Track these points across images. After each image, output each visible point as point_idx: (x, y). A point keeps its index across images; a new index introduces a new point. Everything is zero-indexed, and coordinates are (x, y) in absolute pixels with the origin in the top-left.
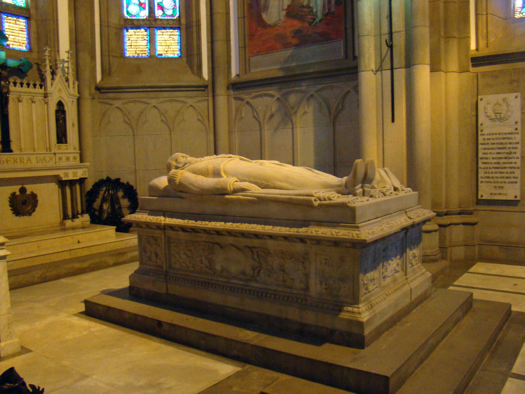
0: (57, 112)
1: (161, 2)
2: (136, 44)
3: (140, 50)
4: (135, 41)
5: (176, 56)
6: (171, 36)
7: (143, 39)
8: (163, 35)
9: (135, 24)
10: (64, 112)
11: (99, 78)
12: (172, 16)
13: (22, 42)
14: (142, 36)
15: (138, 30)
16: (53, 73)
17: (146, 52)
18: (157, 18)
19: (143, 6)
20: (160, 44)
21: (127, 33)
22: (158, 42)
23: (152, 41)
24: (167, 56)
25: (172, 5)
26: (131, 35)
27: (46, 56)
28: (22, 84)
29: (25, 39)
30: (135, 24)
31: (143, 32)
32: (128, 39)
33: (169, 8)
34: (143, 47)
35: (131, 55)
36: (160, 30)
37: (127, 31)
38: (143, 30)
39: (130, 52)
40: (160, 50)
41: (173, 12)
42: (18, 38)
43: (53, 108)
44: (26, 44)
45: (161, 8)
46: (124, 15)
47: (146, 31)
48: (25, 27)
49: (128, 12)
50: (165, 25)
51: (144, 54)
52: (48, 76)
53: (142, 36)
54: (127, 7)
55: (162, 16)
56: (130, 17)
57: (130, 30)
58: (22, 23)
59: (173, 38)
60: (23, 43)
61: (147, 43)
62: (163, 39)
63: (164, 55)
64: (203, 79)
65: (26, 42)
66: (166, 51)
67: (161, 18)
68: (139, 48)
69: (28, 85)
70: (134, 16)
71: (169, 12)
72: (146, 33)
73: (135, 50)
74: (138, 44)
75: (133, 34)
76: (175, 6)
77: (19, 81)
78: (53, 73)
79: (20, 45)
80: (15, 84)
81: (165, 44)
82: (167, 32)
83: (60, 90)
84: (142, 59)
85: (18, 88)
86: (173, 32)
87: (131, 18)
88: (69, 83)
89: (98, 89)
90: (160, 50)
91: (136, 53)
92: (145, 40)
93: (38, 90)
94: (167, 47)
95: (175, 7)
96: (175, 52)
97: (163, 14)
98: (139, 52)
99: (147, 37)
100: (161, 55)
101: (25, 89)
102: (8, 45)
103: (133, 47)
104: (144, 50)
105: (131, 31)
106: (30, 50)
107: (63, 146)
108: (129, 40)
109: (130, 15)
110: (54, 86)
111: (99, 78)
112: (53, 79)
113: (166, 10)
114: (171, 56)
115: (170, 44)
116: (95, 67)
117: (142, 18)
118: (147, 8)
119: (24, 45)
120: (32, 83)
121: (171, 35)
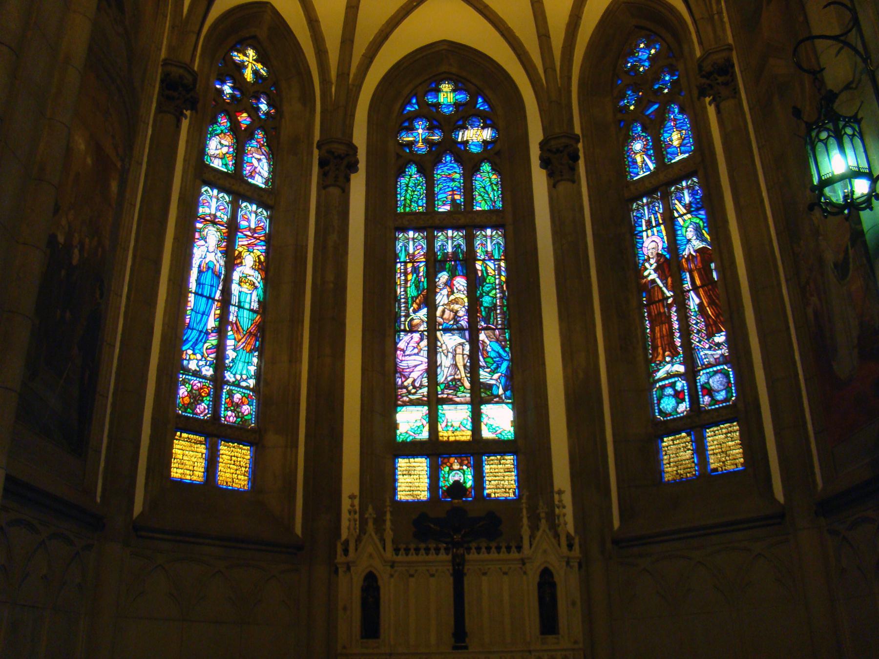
0: (540, 585)
1: (706, 383)
2: (676, 459)
3: (682, 467)
4: (674, 455)
5: (740, 468)
6: (729, 435)
7: (685, 449)
8: (715, 435)
9: (673, 427)
10: (553, 585)
11: (616, 524)
12: (726, 400)
13: (509, 487)
14: (684, 445)
15: (677, 436)
16: (534, 528)
17: (692, 470)
18: (703, 409)
19: (680, 396)
20: (711, 452)
21: (664, 444)
22: (710, 448)
23: (700, 449)
24: (725, 470)
25: (723, 383)
26: (667, 447)
27: (522, 503)
28: (488, 549)
29: (513, 482)
30: (673, 427)
31: (684, 437)
32: (664, 453)
33: (719, 389)
34: (687, 462)
35: (670, 478)
36: (708, 428)
37: (663, 441)
38: (684, 434)
39: (670, 472)
40: (714, 463)
41: (726, 394)
42: (503, 482)
43: (532, 579)
44: (515, 489)
45: (709, 391)
46: (655, 416)
47: (689, 434)
48: (512, 466)
49: (660, 411)
50: (717, 418)
51: (689, 473)
52: (525, 532)
53: (684, 445)
54: (659, 403)
55: (710, 405)
56: (663, 418)
57: (665, 439)
58: (508, 462)
59: (732, 438)
60: (509, 489)
61: (693, 454)
62: (715, 442)
63: (720, 469)
64: (776, 501)
65: (515, 486)
66: (723, 462)
67: (710, 408)
68: (681, 465)
69: (509, 549)
70: (670, 415)
71: (721, 396)
72: (689, 438)
73: (675, 469)
74: (679, 458)
75: (671, 443)
76: (729, 382)
77: (483, 545)
78: (534, 528)
79: (505, 492)
80: (478, 549)
81: (720, 450)
82: (721, 429)
83: (545, 551)
84: (688, 481)
85: (484, 556)
86: (730, 427)
87: (665, 419)
88: (559, 541)
89: (615, 542)
90: (714, 463)
91: (677, 474)
92: (688, 449)
93: (515, 555)
94: (723, 455)
95: (728, 385)
96: (737, 461)
97: (711, 401)
98: (682, 472)
99: (692, 445)
100: (716, 470)
101: (494, 555)
102: (489, 495)
103: (672, 464)
104: (689, 466)
105: (667, 441)
106: (519, 497)
107: (551, 638)
108: (666, 454)
109: (663, 415)
110: (534, 546)
111: (616, 524)
112: (532, 537)
113: (716, 394)
114: (731, 468)
115: (728, 449)
116: (610, 508)
117: (682, 415)
118: (687, 397)
119: (511, 491)
120: (503, 545)
121: (729, 433)
